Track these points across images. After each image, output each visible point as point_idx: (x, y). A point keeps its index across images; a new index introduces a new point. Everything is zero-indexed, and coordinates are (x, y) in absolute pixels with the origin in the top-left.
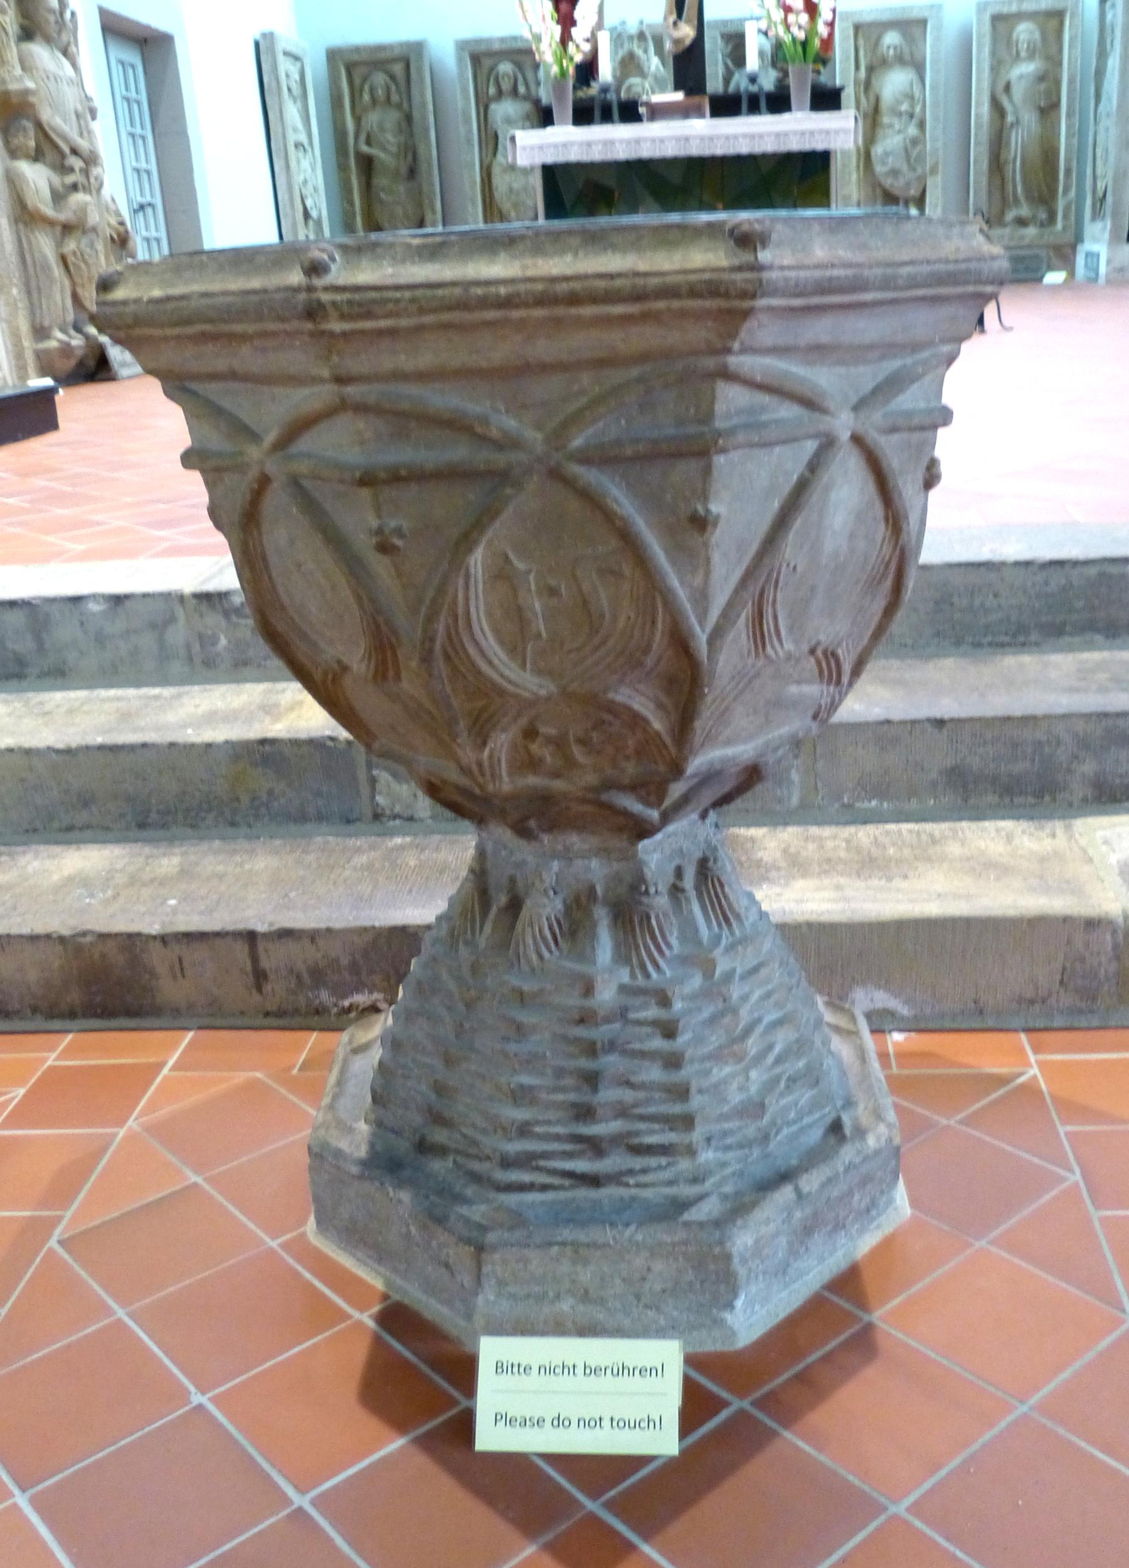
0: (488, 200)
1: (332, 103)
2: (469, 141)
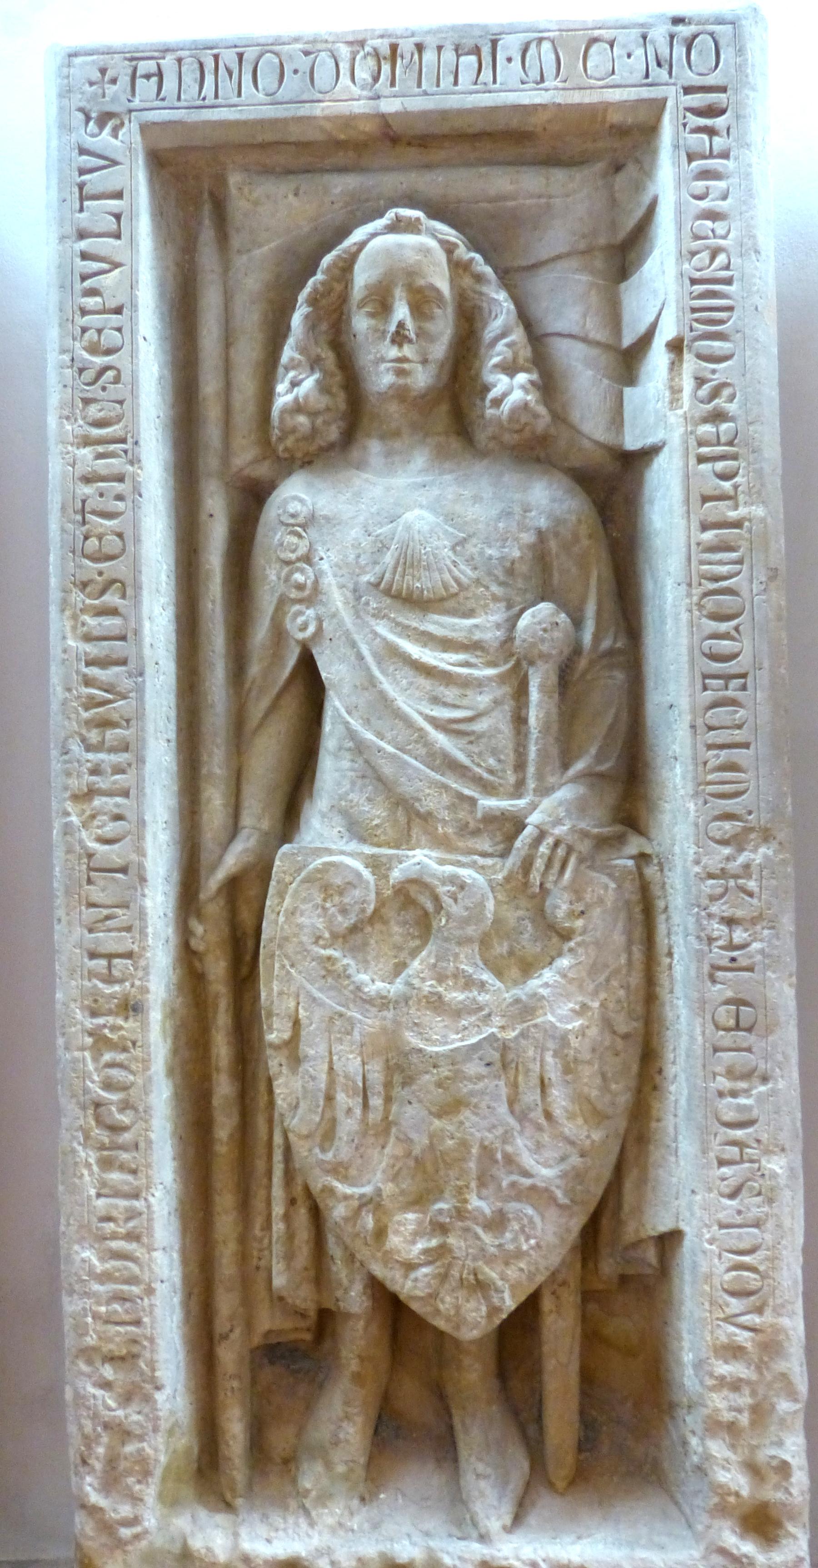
0: (224, 1129)
2: (107, 720)
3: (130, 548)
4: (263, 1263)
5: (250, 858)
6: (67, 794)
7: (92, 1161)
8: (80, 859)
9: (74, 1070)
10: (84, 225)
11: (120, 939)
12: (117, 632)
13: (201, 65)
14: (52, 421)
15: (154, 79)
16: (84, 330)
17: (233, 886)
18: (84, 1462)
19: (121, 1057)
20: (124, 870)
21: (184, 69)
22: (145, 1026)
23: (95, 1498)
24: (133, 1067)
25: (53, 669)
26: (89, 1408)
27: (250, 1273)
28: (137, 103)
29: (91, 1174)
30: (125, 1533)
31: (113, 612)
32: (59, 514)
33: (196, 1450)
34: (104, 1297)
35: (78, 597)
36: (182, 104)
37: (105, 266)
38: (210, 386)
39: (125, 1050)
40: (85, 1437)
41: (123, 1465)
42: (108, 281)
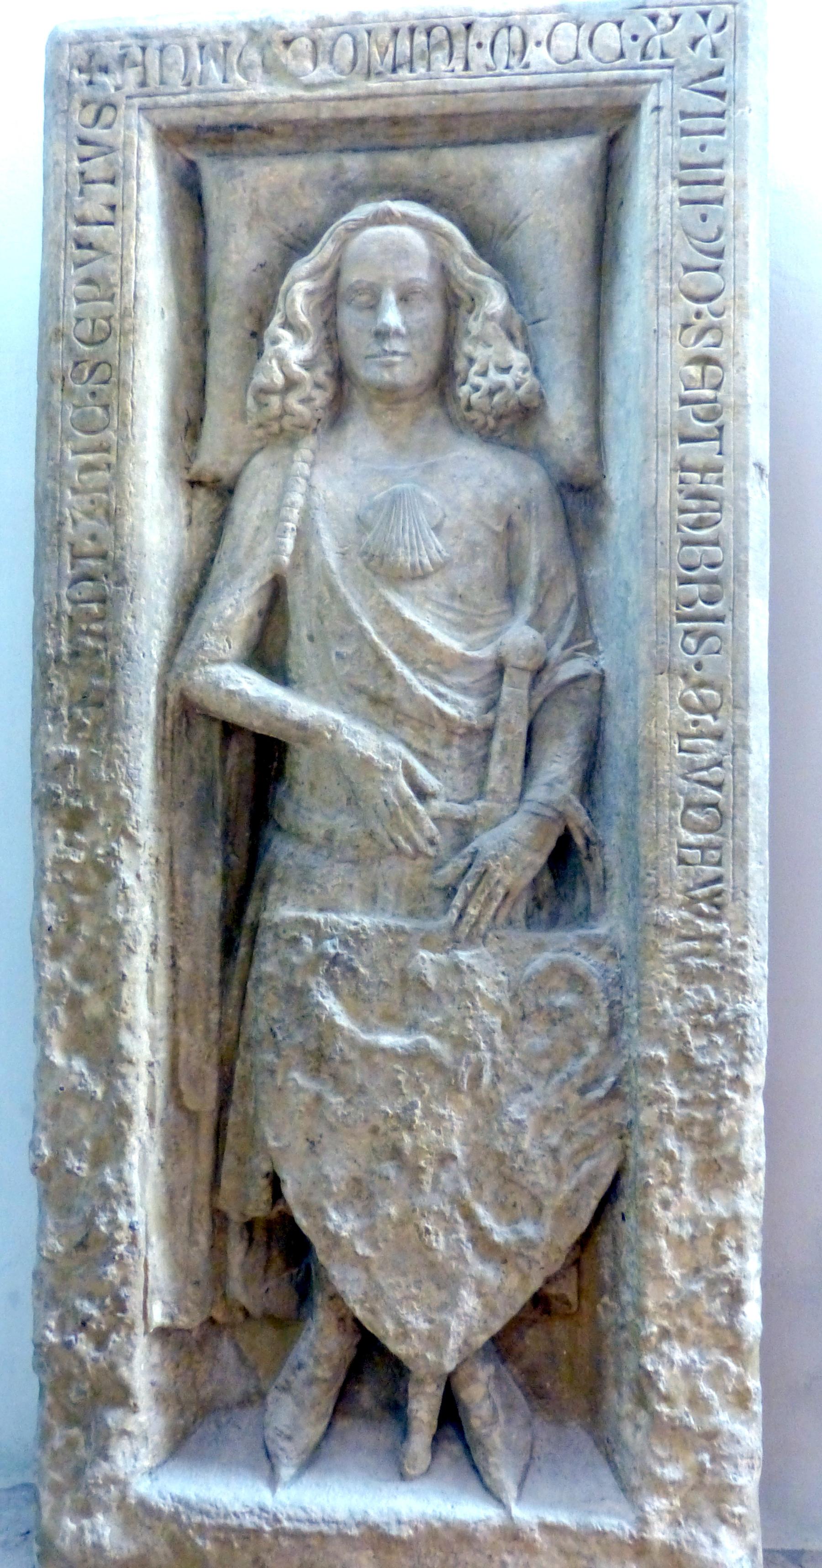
1: (49, 378)
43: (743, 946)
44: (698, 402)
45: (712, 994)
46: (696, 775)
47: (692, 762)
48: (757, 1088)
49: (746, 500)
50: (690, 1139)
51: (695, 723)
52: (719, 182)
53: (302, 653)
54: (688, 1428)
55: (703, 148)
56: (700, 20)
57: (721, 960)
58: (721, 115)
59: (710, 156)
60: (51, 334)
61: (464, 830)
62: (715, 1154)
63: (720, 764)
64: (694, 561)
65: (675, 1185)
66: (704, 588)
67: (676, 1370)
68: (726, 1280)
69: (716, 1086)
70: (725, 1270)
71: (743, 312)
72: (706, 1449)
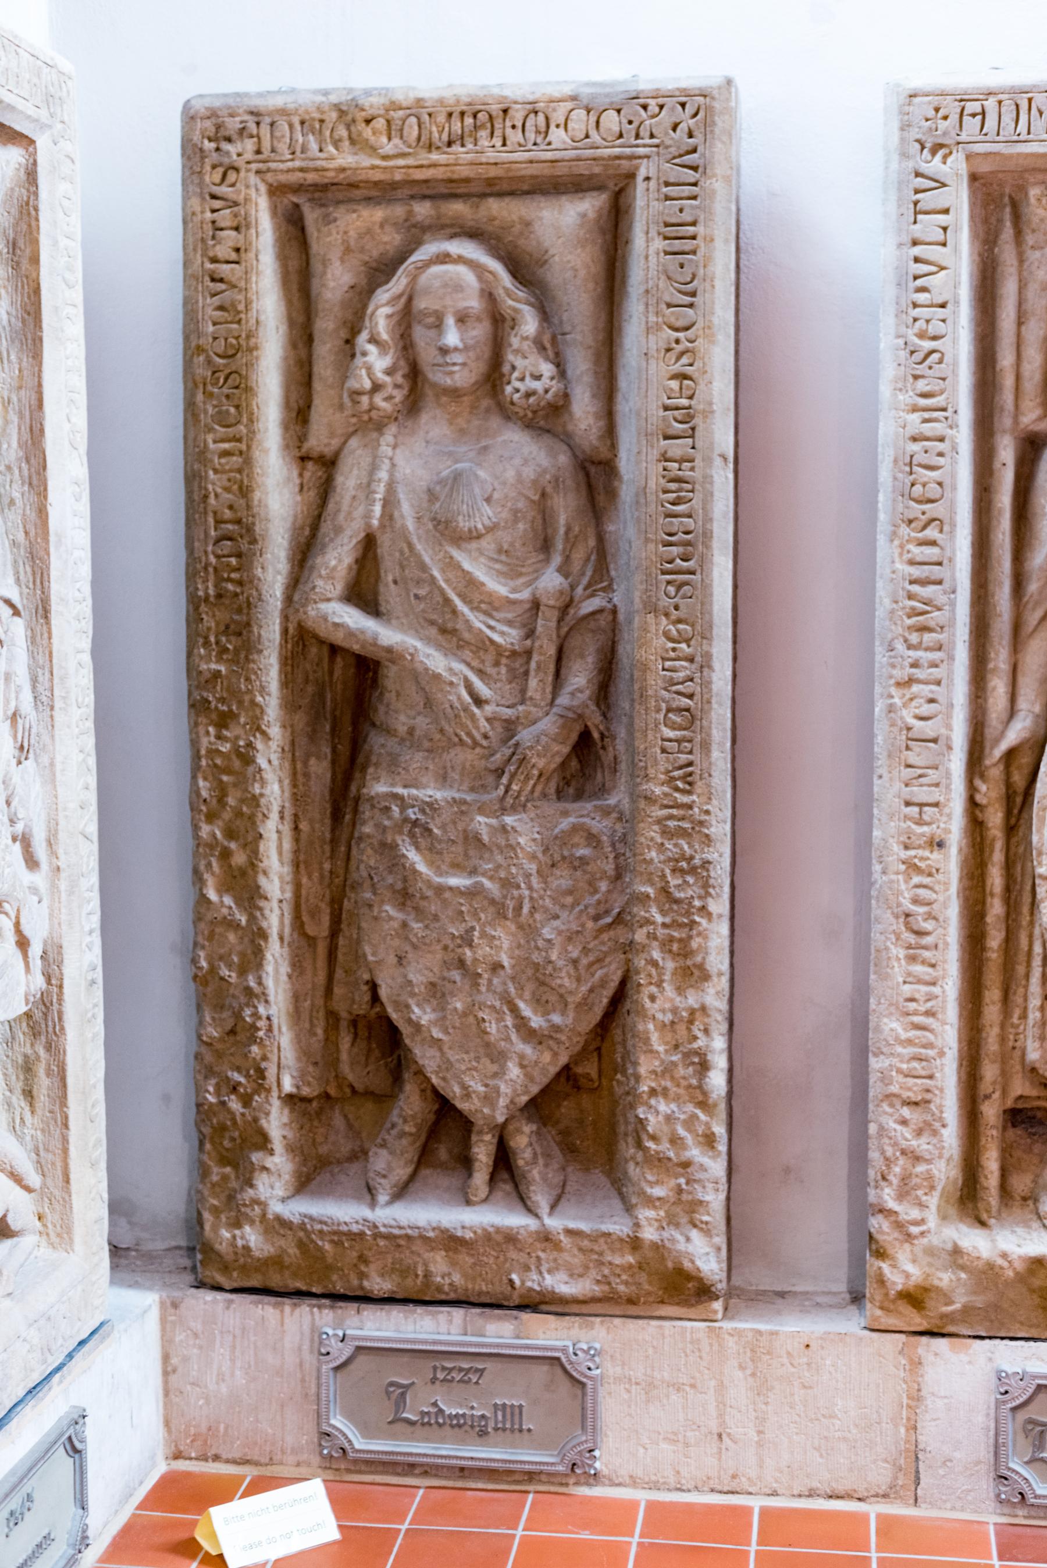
1: (192, 384)
2: (922, 624)
3: (948, 494)
4: (1018, 1044)
5: (1025, 734)
6: (892, 681)
7: (901, 956)
8: (901, 730)
9: (891, 889)
10: (918, 235)
11: (931, 792)
12: (935, 559)
13: (1017, 106)
14: (885, 390)
15: (979, 117)
16: (915, 320)
17: (1010, 754)
18: (884, 1178)
19: (927, 880)
20: (935, 741)
21: (1003, 110)
22: (947, 858)
23: (891, 1204)
24: (937, 888)
25: (880, 584)
26: (890, 1138)
27: (1010, 1052)
28: (964, 137)
29: (900, 966)
30: (914, 1230)
31: (933, 543)
32: (891, 465)
33: (960, 1182)
34: (907, 1058)
35: (904, 531)
36: (1001, 138)
37: (934, 269)
38: (1006, 359)
39: (930, 875)
40: (887, 1159)
41: (915, 1181)
42: (935, 281)
43: (707, 812)
44: (677, 408)
45: (686, 847)
46: (674, 688)
47: (672, 678)
48: (720, 916)
49: (712, 483)
50: (670, 951)
51: (674, 650)
52: (694, 238)
53: (390, 594)
54: (669, 1159)
55: (681, 211)
56: (680, 108)
57: (692, 822)
58: (695, 184)
59: (686, 217)
60: (192, 350)
61: (510, 727)
62: (689, 963)
63: (691, 680)
64: (674, 529)
65: (659, 984)
66: (681, 549)
67: (661, 1118)
68: (696, 1053)
69: (688, 913)
70: (695, 1045)
71: (711, 339)
72: (682, 1175)
